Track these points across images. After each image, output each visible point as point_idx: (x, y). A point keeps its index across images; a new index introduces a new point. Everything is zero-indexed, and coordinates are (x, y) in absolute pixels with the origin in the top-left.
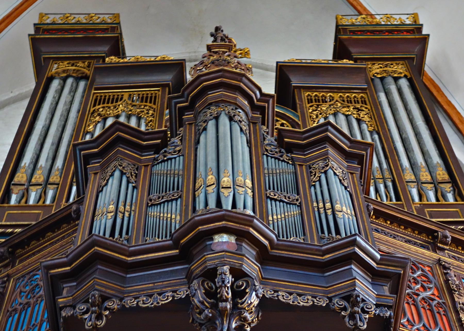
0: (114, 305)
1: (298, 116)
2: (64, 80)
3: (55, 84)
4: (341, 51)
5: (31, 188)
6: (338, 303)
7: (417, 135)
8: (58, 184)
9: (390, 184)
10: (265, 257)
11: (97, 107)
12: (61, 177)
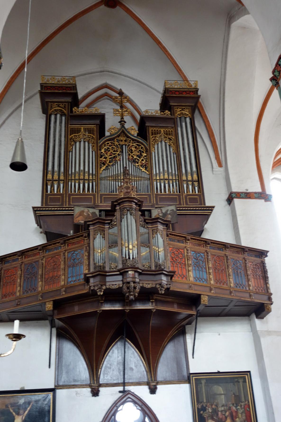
0: (104, 287)
1: (147, 145)
2: (56, 115)
3: (53, 117)
4: (165, 104)
5: (54, 182)
6: (158, 286)
7: (189, 152)
8: (64, 180)
9: (177, 183)
10: (140, 274)
11: (72, 135)
12: (64, 177)
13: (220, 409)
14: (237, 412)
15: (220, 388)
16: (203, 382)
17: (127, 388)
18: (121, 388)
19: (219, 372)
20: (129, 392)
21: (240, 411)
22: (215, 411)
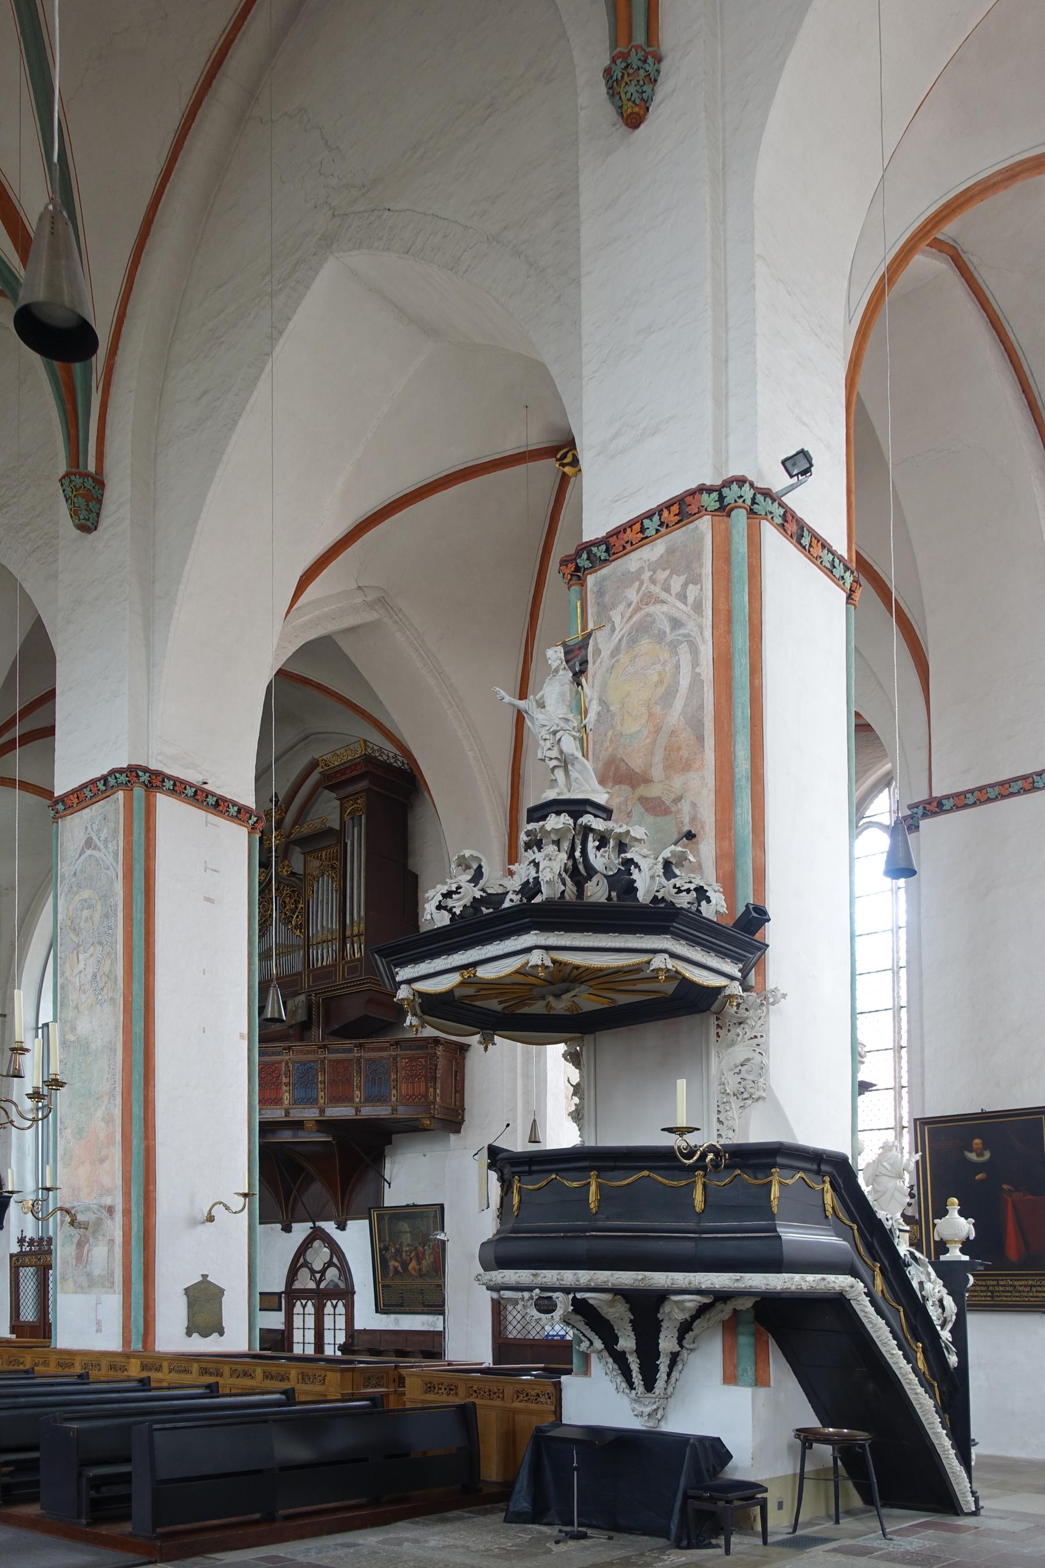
13: (404, 1249)
14: (424, 1253)
15: (406, 1225)
16: (386, 1218)
17: (318, 1224)
18: (311, 1224)
19: (414, 1206)
20: (320, 1228)
21: (428, 1252)
22: (399, 1252)
